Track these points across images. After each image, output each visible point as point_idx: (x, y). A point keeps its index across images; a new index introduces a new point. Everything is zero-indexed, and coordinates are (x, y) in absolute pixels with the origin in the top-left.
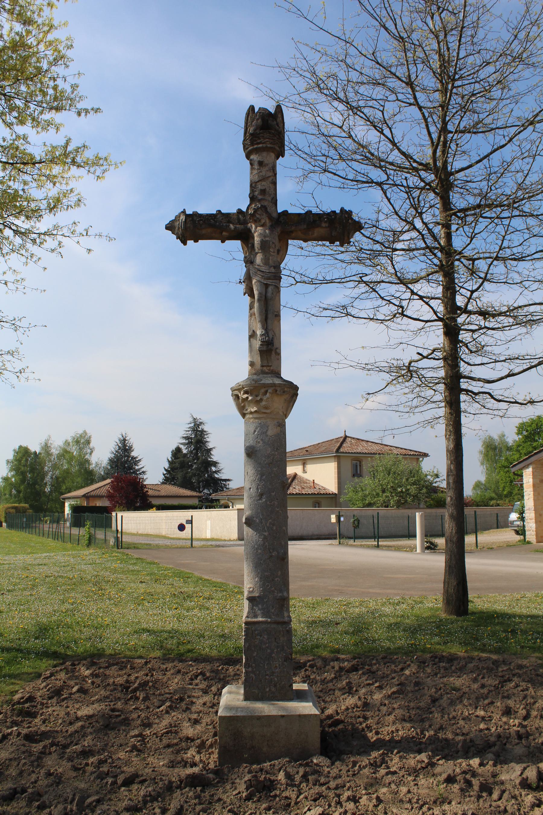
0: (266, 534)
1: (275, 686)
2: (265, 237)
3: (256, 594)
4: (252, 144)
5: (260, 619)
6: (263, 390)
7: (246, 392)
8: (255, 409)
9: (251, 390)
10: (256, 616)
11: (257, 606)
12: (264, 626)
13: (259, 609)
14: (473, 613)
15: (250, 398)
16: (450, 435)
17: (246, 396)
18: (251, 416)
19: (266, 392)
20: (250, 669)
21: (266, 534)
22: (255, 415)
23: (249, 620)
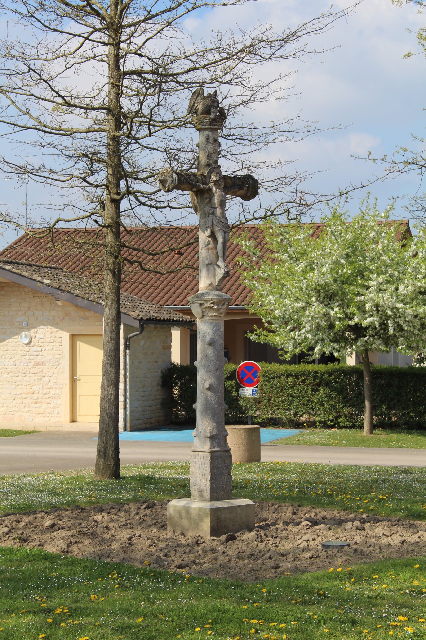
0: (219, 394)
1: (224, 491)
2: (222, 197)
3: (214, 433)
4: (210, 124)
5: (217, 449)
6: (223, 303)
7: (212, 303)
8: (216, 314)
9: (217, 302)
10: (214, 448)
11: (214, 441)
12: (219, 453)
13: (216, 443)
14: (124, 478)
15: (215, 307)
16: (112, 303)
17: (212, 305)
18: (211, 318)
19: (223, 304)
20: (213, 481)
21: (219, 394)
22: (214, 318)
23: (212, 450)
